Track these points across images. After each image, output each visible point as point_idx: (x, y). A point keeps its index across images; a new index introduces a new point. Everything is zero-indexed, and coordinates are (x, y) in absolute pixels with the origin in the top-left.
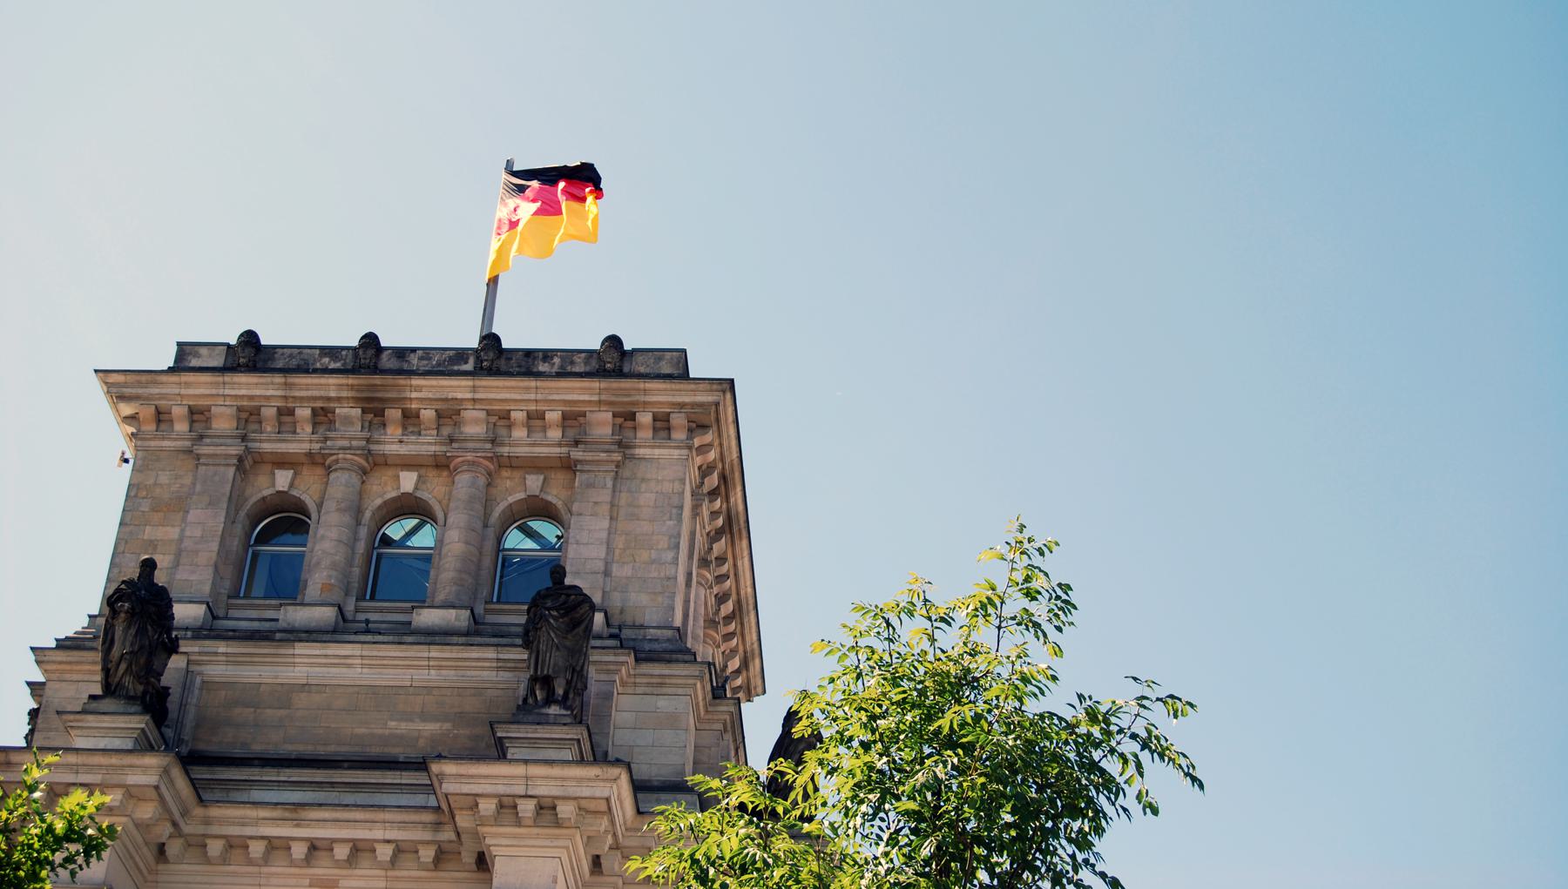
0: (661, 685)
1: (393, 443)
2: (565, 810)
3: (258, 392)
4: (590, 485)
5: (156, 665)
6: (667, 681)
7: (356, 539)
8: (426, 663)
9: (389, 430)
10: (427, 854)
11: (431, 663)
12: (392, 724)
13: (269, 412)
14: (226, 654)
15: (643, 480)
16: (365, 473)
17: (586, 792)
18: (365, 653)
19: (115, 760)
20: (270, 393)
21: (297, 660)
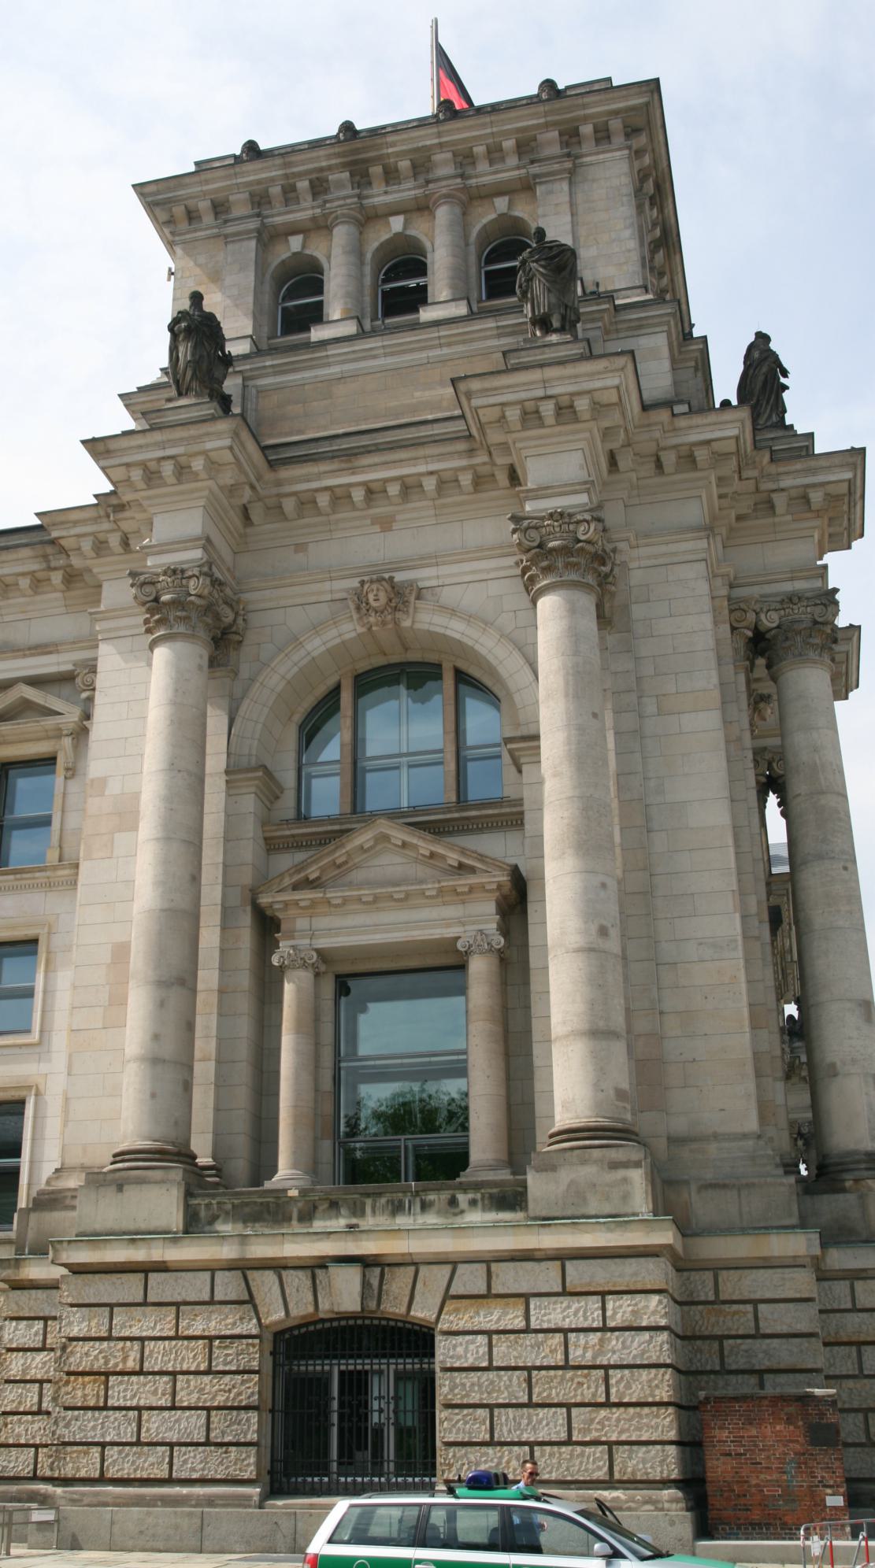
0: (640, 327)
1: (379, 195)
2: (582, 404)
3: (264, 176)
4: (551, 192)
5: (217, 374)
6: (645, 322)
7: (362, 275)
8: (437, 342)
9: (375, 185)
10: (466, 479)
11: (442, 341)
12: (417, 394)
13: (275, 190)
14: (272, 366)
15: (594, 180)
16: (362, 225)
17: (598, 384)
18: (385, 343)
19: (193, 431)
20: (274, 174)
21: (331, 360)
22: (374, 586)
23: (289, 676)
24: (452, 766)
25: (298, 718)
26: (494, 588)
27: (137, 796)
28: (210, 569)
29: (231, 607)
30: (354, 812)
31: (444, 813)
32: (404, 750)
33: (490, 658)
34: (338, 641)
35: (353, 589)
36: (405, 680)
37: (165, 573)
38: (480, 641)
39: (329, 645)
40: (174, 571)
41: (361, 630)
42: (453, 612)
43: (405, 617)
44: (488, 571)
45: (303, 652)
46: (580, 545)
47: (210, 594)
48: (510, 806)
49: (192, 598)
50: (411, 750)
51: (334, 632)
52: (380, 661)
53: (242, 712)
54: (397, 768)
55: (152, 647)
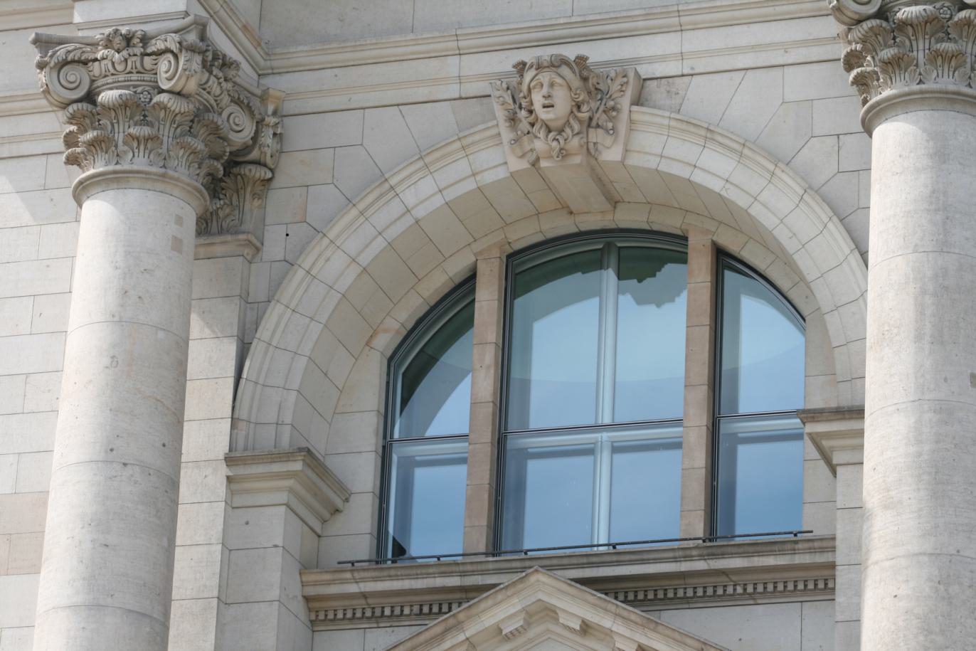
22: (545, 77)
23: (365, 259)
24: (700, 459)
25: (386, 341)
26: (797, 84)
27: (41, 500)
28: (203, 37)
29: (249, 109)
30: (495, 548)
31: (675, 560)
32: (607, 421)
33: (782, 235)
34: (470, 185)
35: (501, 76)
36: (613, 260)
37: (108, 43)
38: (764, 197)
39: (451, 194)
40: (128, 39)
41: (517, 164)
42: (709, 134)
43: (608, 140)
44: (785, 47)
45: (395, 208)
46: (963, 14)
47: (203, 86)
48: (812, 551)
49: (164, 98)
50: (617, 421)
51: (462, 167)
52: (564, 226)
53: (264, 332)
54: (589, 451)
55: (81, 191)
